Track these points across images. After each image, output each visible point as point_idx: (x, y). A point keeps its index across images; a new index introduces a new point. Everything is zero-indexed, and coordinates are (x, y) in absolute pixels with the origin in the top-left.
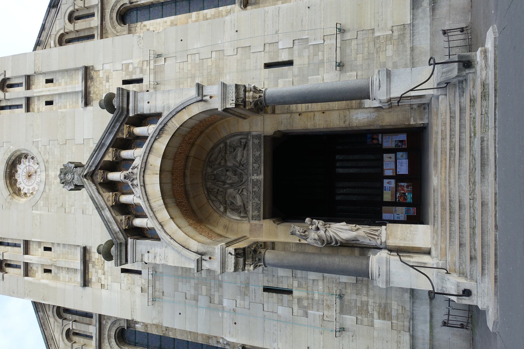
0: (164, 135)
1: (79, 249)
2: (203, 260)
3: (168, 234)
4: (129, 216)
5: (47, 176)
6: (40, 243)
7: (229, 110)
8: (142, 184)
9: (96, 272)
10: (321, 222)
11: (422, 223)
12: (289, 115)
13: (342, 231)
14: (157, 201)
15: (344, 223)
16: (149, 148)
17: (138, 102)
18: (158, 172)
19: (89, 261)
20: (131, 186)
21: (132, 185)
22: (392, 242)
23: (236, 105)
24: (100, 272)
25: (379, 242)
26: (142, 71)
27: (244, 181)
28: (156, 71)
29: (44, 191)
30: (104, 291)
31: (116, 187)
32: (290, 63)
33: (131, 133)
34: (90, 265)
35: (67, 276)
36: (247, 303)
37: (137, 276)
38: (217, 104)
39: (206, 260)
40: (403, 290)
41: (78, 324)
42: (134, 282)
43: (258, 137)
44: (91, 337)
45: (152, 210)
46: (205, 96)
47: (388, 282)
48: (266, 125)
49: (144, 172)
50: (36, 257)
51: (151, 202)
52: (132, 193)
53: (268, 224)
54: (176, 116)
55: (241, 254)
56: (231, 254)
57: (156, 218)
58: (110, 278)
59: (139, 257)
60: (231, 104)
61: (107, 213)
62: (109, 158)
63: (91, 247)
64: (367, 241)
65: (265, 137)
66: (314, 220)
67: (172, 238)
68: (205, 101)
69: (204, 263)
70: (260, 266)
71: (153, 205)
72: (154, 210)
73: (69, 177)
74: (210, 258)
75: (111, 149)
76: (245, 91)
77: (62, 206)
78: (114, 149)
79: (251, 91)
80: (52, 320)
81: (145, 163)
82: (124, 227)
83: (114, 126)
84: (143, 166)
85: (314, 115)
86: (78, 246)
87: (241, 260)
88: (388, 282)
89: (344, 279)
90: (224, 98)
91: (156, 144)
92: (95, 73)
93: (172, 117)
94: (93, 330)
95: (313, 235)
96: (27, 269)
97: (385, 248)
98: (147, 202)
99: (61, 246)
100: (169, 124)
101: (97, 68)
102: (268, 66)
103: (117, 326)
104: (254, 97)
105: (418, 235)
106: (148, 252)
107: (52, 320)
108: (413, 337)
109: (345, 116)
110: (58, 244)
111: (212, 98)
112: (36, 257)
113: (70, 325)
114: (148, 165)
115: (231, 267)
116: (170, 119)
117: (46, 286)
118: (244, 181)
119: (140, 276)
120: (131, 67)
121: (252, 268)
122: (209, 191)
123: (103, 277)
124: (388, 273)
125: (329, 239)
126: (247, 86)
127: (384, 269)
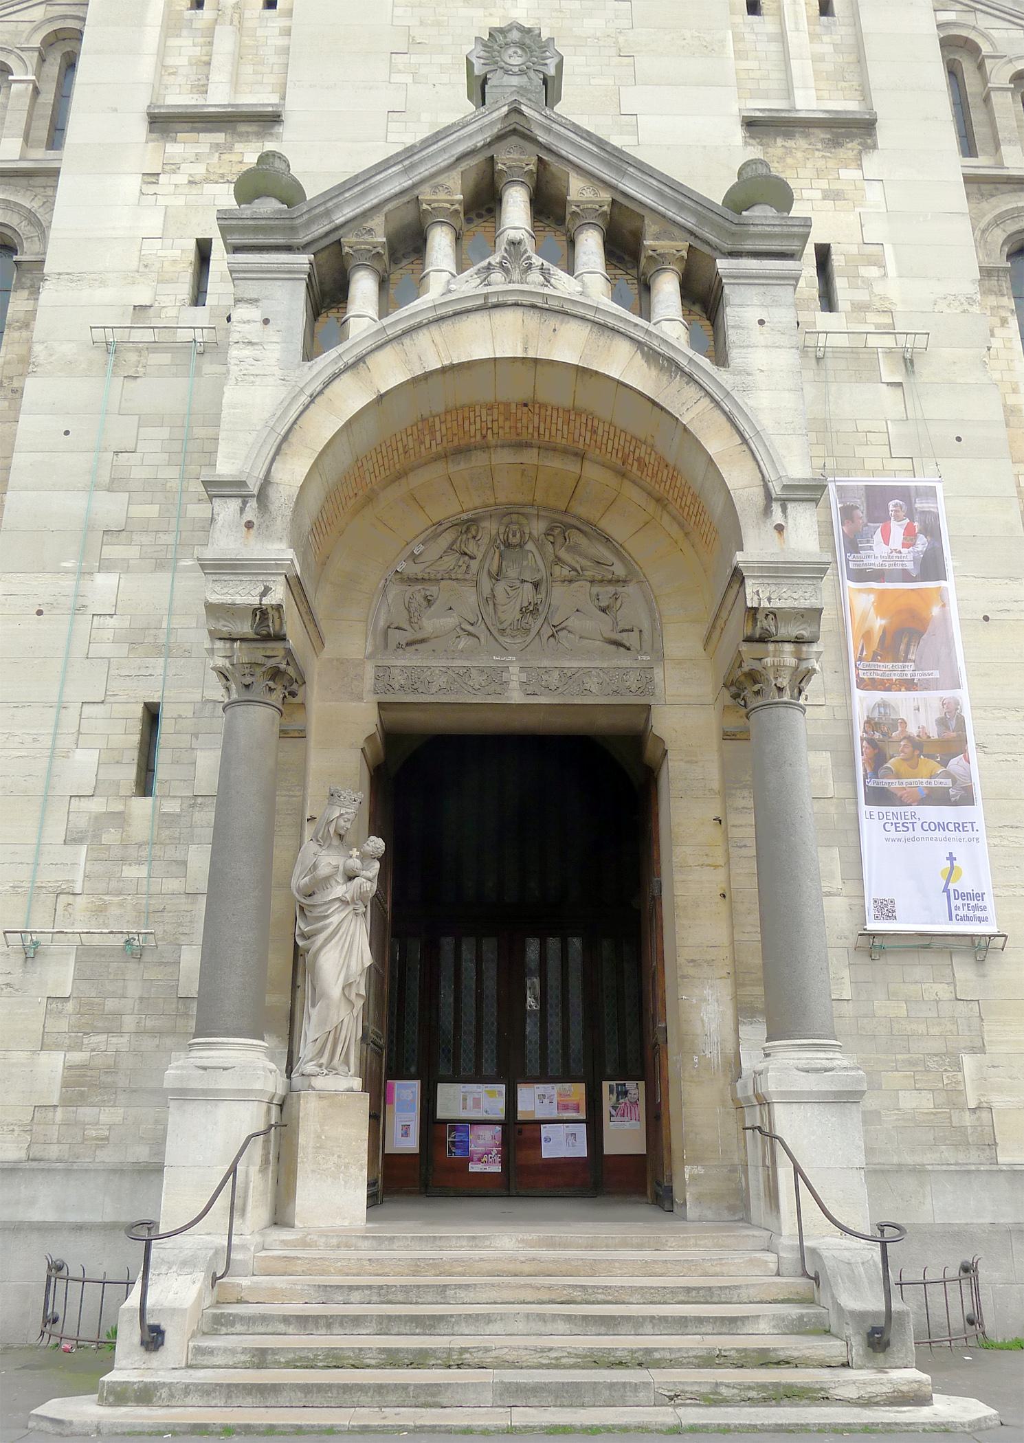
0: (654, 372)
1: (274, 99)
2: (245, 503)
3: (327, 384)
4: (386, 258)
7: (736, 586)
8: (493, 300)
9: (198, 158)
10: (371, 887)
11: (374, 1199)
12: (716, 785)
13: (345, 956)
14: (431, 352)
15: (368, 959)
16: (611, 322)
17: (762, 289)
18: (531, 355)
19: (234, 132)
20: (484, 263)
21: (489, 268)
22: (309, 1110)
23: (754, 611)
24: (200, 170)
25: (310, 1068)
27: (501, 639)
31: (480, 216)
34: (220, 137)
35: (184, 61)
36: (106, 650)
37: (185, 288)
38: (756, 547)
39: (242, 510)
40: (159, 1142)
41: (27, 100)
42: (167, 282)
43: (647, 685)
45: (405, 333)
46: (784, 510)
47: (184, 1095)
49: (533, 306)
51: (434, 328)
52: (461, 267)
54: (718, 413)
55: (264, 626)
56: (264, 594)
57: (379, 348)
58: (180, 201)
59: (251, 289)
60: (756, 593)
63: (279, 137)
64: (311, 1030)
65: (648, 707)
66: (377, 865)
67: (313, 398)
68: (767, 511)
69: (234, 504)
70: (228, 689)
71: (423, 339)
72: (407, 341)
74: (249, 525)
75: (606, 196)
76: (799, 641)
77: (413, 42)
78: (606, 208)
79: (800, 659)
81: (560, 311)
82: (350, 240)
83: (682, 207)
84: (553, 304)
85: (716, 867)
86: (283, 98)
87: (246, 628)
89: (191, 957)
91: (623, 349)
92: (851, 154)
93: (713, 400)
95: (329, 861)
97: (290, 1089)
98: (431, 315)
99: (282, 41)
100: (691, 392)
103: (23, 228)
104: (778, 669)
106: (266, 321)
109: (710, 963)
110: (287, 32)
111: (775, 534)
114: (553, 321)
115: (223, 593)
116: (708, 394)
118: (501, 639)
119: (188, 302)
121: (221, 662)
122: (468, 526)
123: (181, 179)
124: (210, 1096)
125: (317, 912)
126: (814, 648)
127: (224, 1082)
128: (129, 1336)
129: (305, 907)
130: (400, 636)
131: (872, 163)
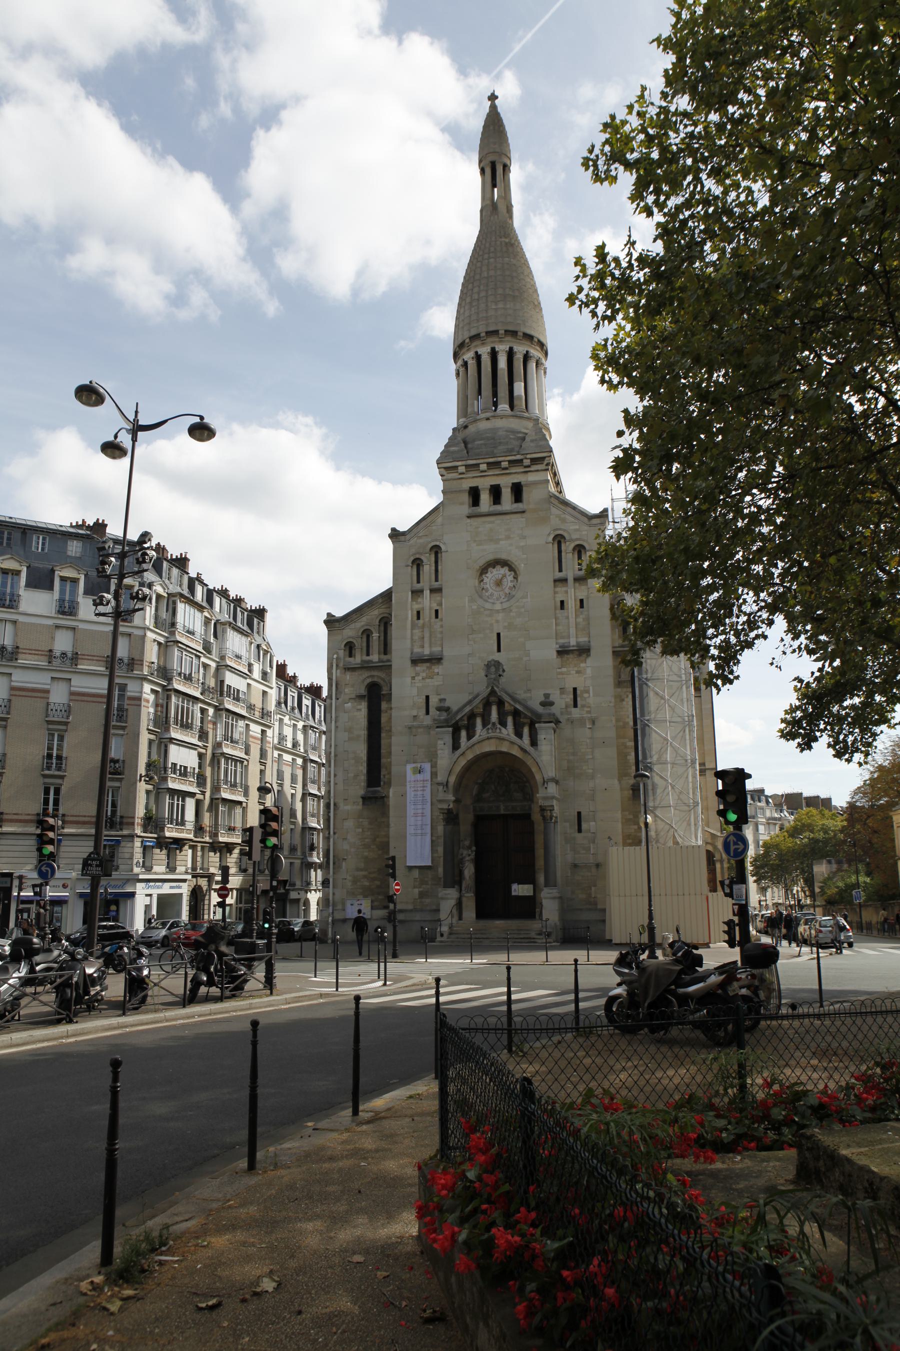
5: (498, 611)
6: (440, 604)
13: (469, 871)
22: (464, 899)
24: (424, 675)
26: (583, 706)
28: (582, 722)
29: (486, 610)
30: (409, 680)
32: (580, 831)
33: (524, 725)
40: (439, 905)
43: (530, 808)
44: (368, 655)
48: (536, 817)
50: (427, 602)
52: (484, 725)
53: (470, 817)
55: (449, 811)
60: (541, 802)
61: (467, 709)
62: (507, 707)
73: (493, 669)
80: (376, 612)
88: (442, 899)
90: (546, 798)
94: (375, 657)
95: (465, 852)
96: (417, 593)
101: (589, 660)
102: (579, 814)
103: (382, 683)
105: (470, 913)
107: (376, 612)
108: (411, 911)
112: (427, 602)
113: (375, 635)
115: (440, 806)
117: (407, 618)
120: (586, 695)
128: (438, 935)
129: (462, 861)
130: (478, 799)
131: (589, 661)
